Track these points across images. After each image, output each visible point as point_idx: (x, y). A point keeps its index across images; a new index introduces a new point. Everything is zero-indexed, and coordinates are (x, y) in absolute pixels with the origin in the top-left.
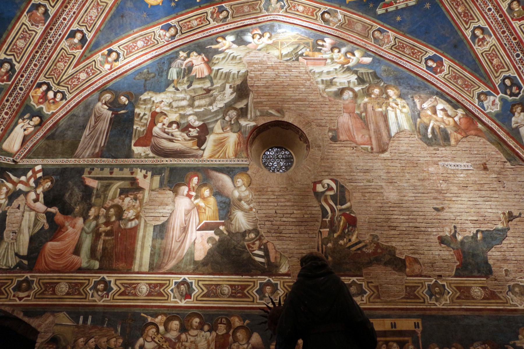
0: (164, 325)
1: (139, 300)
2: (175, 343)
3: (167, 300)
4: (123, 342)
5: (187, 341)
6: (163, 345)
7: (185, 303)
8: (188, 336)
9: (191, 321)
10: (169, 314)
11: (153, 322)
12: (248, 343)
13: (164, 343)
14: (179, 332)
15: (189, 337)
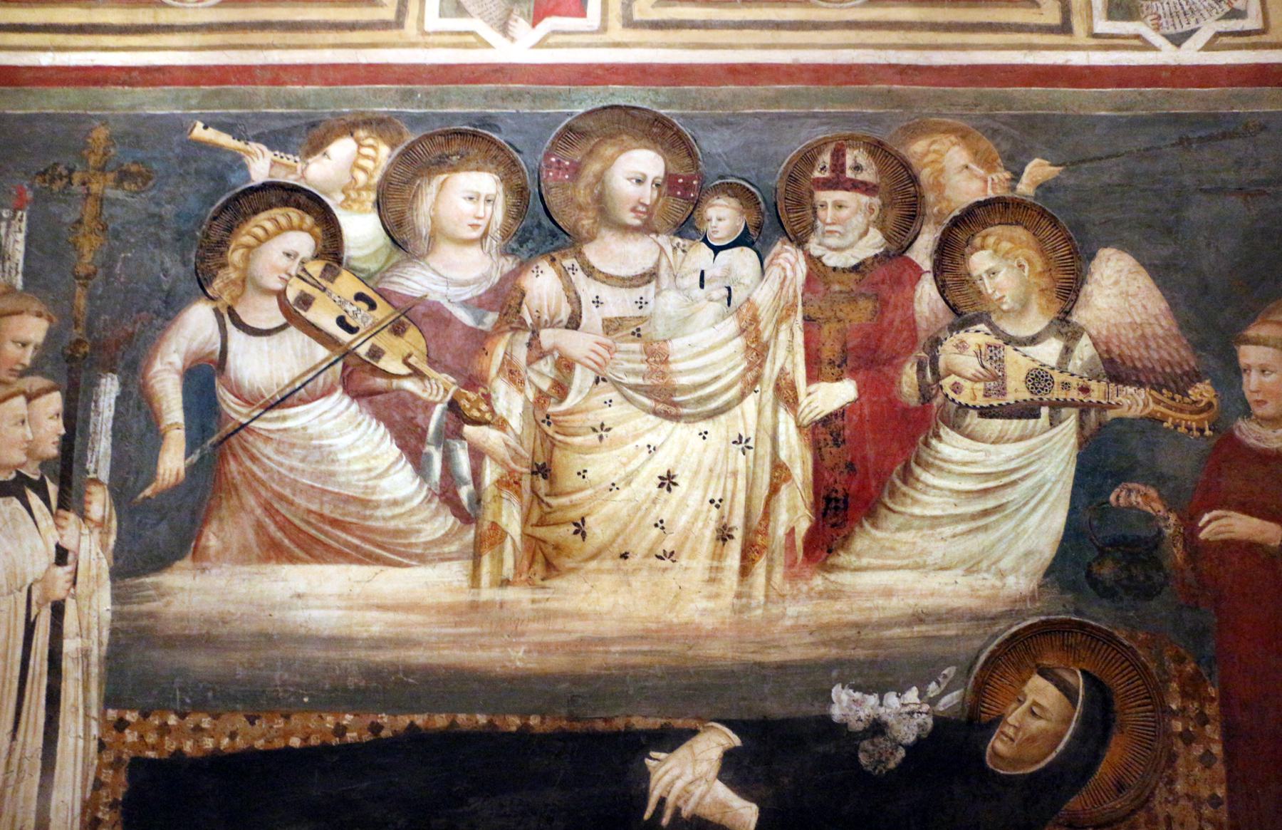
0: (379, 205)
1: (170, 29)
2: (479, 341)
3: (398, 24)
4: (51, 336)
5: (574, 323)
6: (376, 353)
7: (541, 44)
8: (580, 278)
9: (594, 167)
10: (415, 121)
11: (291, 180)
12: (1064, 326)
13: (385, 340)
14: (506, 252)
15: (587, 289)
